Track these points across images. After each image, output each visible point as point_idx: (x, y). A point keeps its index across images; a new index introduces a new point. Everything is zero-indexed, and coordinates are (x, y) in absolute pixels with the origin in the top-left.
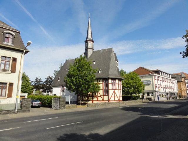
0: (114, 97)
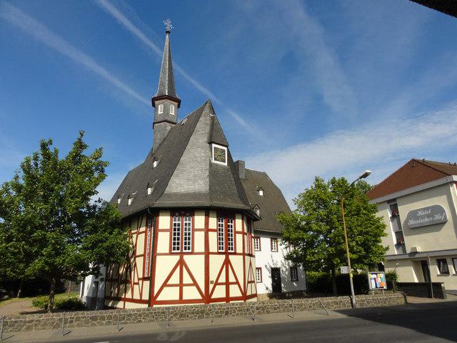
0: (181, 285)
